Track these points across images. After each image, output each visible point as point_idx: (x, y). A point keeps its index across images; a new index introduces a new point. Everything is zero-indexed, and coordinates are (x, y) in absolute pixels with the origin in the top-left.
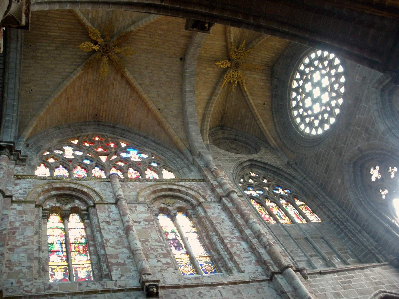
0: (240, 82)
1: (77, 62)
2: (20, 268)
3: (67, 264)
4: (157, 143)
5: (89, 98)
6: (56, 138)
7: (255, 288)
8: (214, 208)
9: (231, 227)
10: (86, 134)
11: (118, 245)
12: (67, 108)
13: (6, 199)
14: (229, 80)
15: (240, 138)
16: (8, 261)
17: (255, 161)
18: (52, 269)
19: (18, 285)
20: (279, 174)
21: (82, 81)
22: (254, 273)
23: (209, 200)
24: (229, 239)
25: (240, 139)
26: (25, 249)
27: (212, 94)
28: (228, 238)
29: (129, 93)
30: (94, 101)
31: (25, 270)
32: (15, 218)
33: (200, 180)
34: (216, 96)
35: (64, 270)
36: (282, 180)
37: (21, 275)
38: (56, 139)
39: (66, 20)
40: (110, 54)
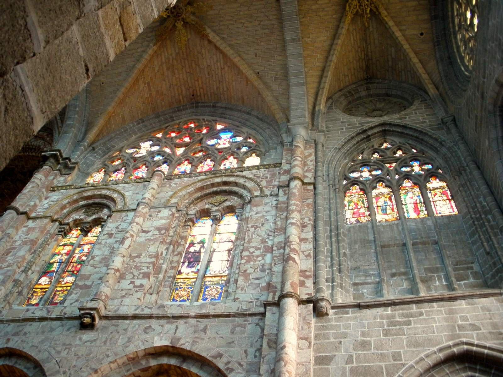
0: (375, 10)
1: (150, 37)
4: (261, 120)
5: (177, 76)
6: (136, 134)
10: (177, 122)
12: (151, 95)
13: (20, 216)
14: (355, 10)
15: (394, 92)
17: (390, 124)
20: (422, 140)
21: (161, 58)
23: (268, 193)
25: (393, 93)
27: (335, 37)
29: (222, 61)
30: (185, 79)
34: (338, 39)
36: (426, 150)
38: (135, 135)
40: (183, 16)
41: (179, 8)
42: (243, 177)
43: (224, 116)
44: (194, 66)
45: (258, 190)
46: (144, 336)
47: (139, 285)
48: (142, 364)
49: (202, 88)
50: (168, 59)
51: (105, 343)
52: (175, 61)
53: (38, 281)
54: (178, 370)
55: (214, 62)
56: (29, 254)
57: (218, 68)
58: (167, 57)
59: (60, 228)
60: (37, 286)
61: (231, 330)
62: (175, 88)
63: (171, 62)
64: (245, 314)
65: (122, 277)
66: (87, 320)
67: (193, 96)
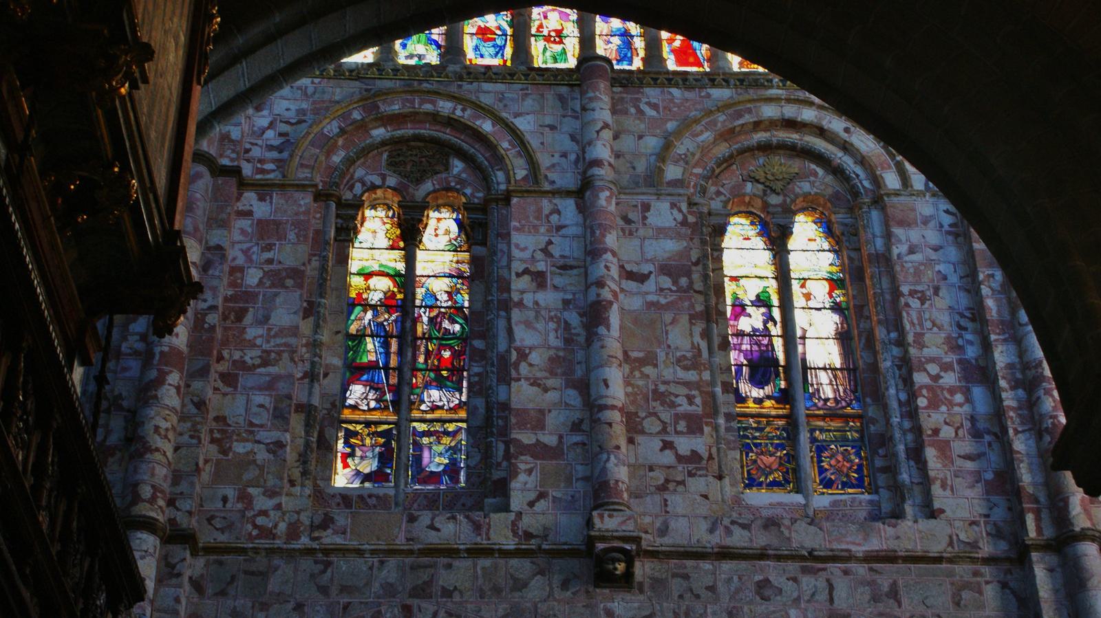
2: (249, 446)
3: (393, 418)
7: (952, 584)
9: (957, 317)
11: (553, 373)
16: (217, 419)
18: (349, 435)
19: (240, 506)
22: (973, 523)
24: (933, 369)
26: (268, 378)
31: (262, 455)
32: (246, 252)
35: (381, 440)
37: (249, 475)
45: (890, 167)
47: (688, 453)
64: (975, 558)
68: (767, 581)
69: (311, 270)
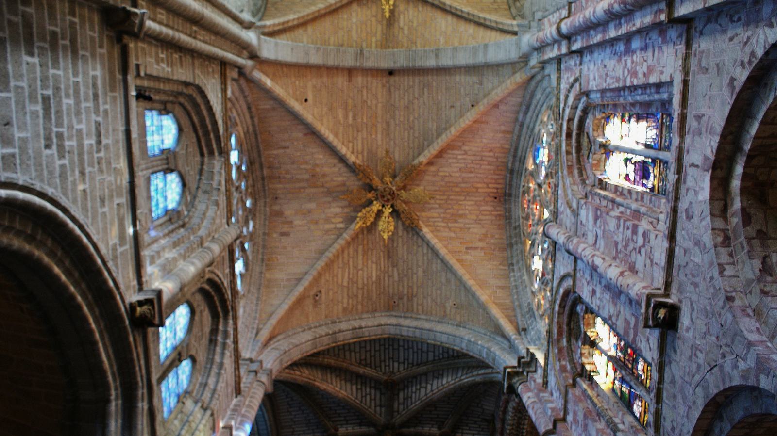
4: (528, 107)
5: (467, 212)
8: (588, 69)
12: (482, 249)
28: (626, 75)
30: (473, 203)
33: (559, 70)
39: (351, 260)
41: (385, 191)
42: (564, 110)
43: (522, 158)
44: (458, 189)
46: (696, 219)
48: (737, 223)
49: (487, 184)
50: (444, 218)
51: (696, 285)
52: (448, 211)
53: (635, 417)
54: (754, 162)
55: (455, 163)
56: (598, 423)
57: (465, 159)
58: (441, 220)
59: (585, 377)
60: (642, 420)
61: (703, 73)
62: (481, 217)
63: (448, 216)
65: (633, 269)
66: (662, 313)
67: (496, 198)
68: (687, 210)
69: (590, 406)
